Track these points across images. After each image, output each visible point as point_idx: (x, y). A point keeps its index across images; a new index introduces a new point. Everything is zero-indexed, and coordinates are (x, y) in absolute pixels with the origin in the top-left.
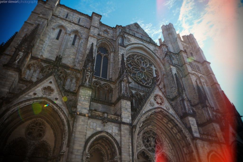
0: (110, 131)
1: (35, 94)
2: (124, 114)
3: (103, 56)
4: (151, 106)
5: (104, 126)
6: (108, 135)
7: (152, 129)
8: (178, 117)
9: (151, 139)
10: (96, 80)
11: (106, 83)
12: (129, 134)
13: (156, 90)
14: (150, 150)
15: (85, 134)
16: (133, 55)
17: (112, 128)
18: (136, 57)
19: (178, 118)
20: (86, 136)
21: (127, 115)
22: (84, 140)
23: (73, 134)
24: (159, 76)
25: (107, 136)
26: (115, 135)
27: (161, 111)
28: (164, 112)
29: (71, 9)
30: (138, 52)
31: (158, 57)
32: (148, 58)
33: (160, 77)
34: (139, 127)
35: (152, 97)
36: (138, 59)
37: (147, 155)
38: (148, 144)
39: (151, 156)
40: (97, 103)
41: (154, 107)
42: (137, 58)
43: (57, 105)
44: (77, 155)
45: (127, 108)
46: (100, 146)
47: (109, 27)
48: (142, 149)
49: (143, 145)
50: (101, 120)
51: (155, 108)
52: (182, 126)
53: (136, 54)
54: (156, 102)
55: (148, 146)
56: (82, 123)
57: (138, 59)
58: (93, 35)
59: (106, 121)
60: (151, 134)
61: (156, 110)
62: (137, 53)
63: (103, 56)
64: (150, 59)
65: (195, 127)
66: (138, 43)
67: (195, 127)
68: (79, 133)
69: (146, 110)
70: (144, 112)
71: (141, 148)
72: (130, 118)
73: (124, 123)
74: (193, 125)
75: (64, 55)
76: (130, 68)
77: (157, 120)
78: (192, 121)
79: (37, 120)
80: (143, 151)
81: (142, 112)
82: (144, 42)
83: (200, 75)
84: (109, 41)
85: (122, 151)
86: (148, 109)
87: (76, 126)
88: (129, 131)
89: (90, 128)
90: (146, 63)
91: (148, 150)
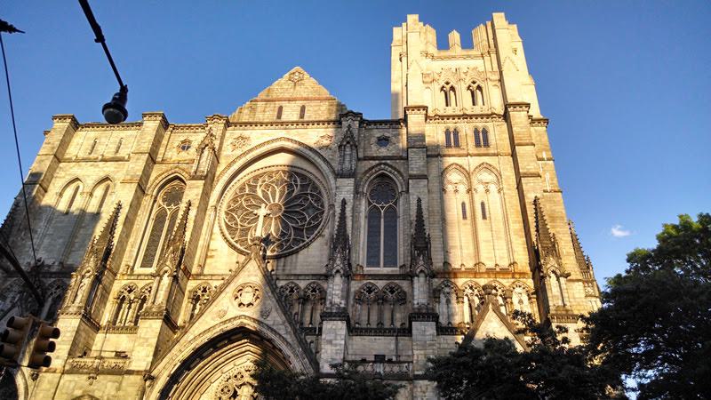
5: (91, 384)
8: (289, 329)
13: (247, 273)
16: (256, 179)
19: (287, 333)
24: (323, 212)
33: (325, 214)
35: (228, 295)
50: (87, 373)
51: (224, 322)
52: (294, 353)
54: (236, 303)
56: (48, 386)
58: (132, 176)
63: (169, 213)
65: (336, 345)
67: (336, 345)
69: (197, 333)
70: (192, 337)
72: (150, 359)
73: (130, 372)
74: (330, 342)
75: (74, 245)
78: (335, 331)
83: (475, 161)
84: (183, 170)
89: (62, 393)
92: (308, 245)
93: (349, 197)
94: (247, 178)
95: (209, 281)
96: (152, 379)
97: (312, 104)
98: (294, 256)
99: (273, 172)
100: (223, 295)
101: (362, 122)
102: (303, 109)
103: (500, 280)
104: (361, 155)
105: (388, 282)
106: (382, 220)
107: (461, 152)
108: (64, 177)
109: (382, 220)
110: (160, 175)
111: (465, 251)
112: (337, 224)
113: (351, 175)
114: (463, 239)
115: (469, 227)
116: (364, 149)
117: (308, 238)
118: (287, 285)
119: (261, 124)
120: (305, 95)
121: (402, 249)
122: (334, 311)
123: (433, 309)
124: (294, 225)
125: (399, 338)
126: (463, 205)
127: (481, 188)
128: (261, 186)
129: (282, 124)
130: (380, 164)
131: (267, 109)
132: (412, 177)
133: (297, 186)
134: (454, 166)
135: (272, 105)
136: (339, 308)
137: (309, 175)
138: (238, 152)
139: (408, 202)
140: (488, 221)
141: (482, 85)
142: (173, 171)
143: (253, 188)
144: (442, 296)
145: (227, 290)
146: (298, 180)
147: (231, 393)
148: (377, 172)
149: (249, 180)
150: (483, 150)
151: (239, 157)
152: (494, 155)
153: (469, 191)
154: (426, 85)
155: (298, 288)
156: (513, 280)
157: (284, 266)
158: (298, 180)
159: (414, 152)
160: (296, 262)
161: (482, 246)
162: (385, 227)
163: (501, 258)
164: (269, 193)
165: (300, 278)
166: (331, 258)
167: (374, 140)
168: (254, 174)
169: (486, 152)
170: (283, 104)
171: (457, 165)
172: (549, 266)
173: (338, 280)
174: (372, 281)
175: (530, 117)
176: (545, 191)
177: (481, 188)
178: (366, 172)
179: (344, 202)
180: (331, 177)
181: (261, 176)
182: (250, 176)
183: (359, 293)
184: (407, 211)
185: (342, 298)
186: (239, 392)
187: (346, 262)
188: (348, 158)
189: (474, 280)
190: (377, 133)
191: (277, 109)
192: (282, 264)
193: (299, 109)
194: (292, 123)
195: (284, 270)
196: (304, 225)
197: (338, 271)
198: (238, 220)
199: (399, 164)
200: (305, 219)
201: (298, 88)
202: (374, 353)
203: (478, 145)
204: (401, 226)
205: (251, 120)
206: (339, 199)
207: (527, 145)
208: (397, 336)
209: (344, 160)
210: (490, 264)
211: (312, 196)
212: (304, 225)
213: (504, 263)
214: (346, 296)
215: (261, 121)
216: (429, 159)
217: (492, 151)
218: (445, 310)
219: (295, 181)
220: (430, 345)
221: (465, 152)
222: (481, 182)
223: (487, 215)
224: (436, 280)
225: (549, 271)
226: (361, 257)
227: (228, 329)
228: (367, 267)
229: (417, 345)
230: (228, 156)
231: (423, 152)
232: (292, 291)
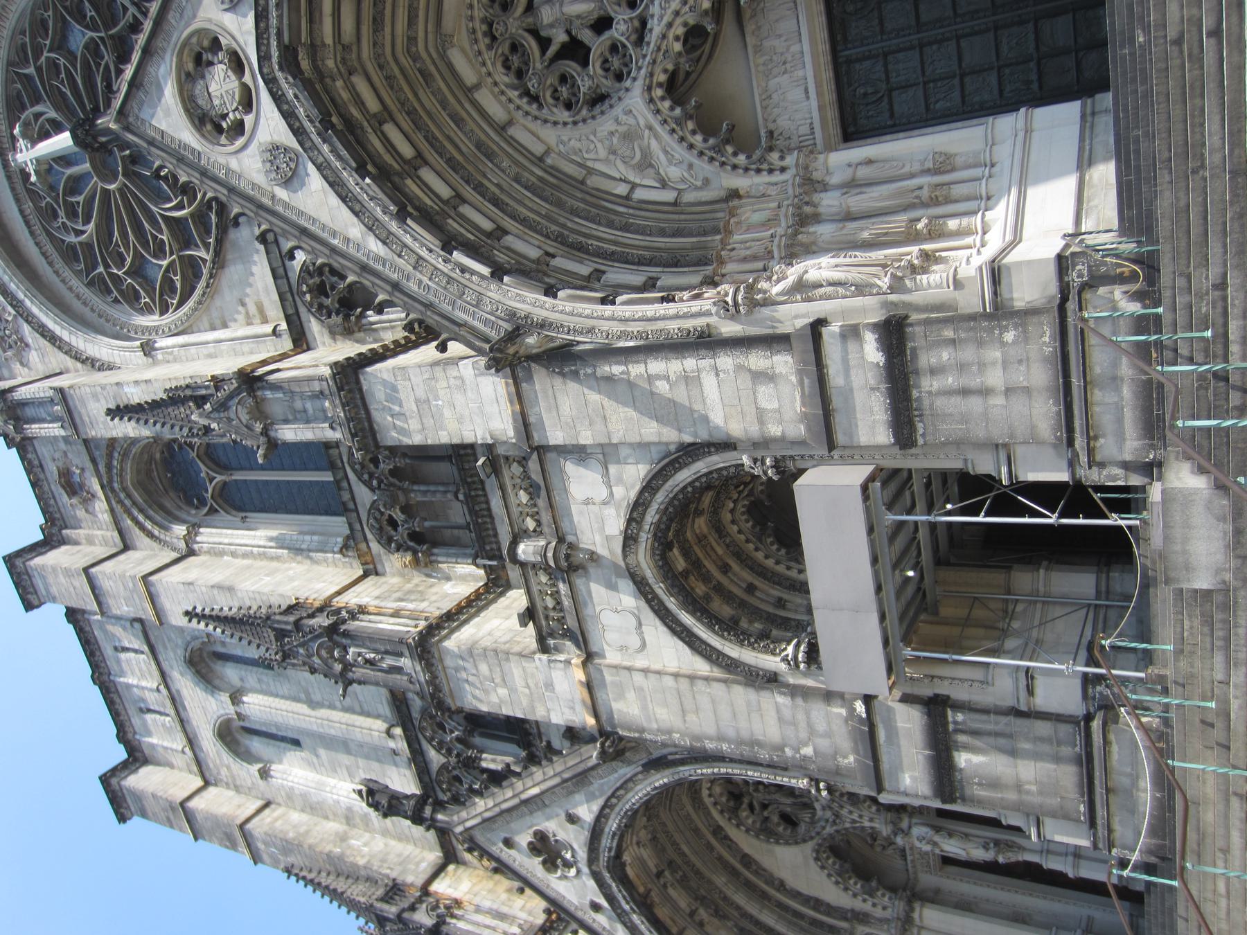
0: (615, 524)
1: (596, 907)
2: (460, 420)
3: (219, 478)
6: (638, 534)
7: (474, 31)
9: (551, 26)
10: (370, 536)
11: (354, 470)
12: (572, 386)
14: (636, 23)
15: (684, 684)
16: (69, 254)
17: (588, 502)
20: (692, 678)
21: (459, 399)
22: (719, 689)
23: (710, 745)
25: (645, 538)
26: (620, 480)
27: (289, 61)
28: (279, 34)
29: (110, 704)
34: (493, 286)
35: (234, 164)
36: (72, 212)
37: (678, 47)
38: (597, 45)
39: (677, 13)
40: (493, 523)
41: (292, 142)
43: (601, 818)
44: (810, 725)
45: (417, 401)
46: (731, 505)
47: (29, 471)
48: (650, 117)
49: (618, 110)
51: (298, 132)
55: (614, 48)
56: (631, 695)
59: (563, 550)
60: (513, 24)
61: (307, 124)
62: (38, 229)
63: (219, 478)
68: (691, 718)
69: (355, 230)
70: (374, 246)
71: (650, 128)
73: (525, 424)
76: (167, 270)
77: (377, 23)
79: (715, 804)
80: (659, 92)
81: (377, 258)
85: (703, 436)
86: (334, 200)
87: (658, 730)
88: (558, 381)
91: (640, 40)
94: (74, 282)
95: (294, 278)
96: (514, 335)
99: (38, 208)
108: (228, 767)
110: (142, 528)
117: (125, 9)
128: (79, 233)
133: (38, 116)
142: (122, 496)
147: (571, 67)
149: (78, 274)
164: (81, 199)
168: (59, 264)
181: (58, 243)
182: (67, 273)
186: (560, 37)
196: (101, 38)
198: (165, 263)
200: (93, 48)
211: (38, 53)
227: (314, 112)
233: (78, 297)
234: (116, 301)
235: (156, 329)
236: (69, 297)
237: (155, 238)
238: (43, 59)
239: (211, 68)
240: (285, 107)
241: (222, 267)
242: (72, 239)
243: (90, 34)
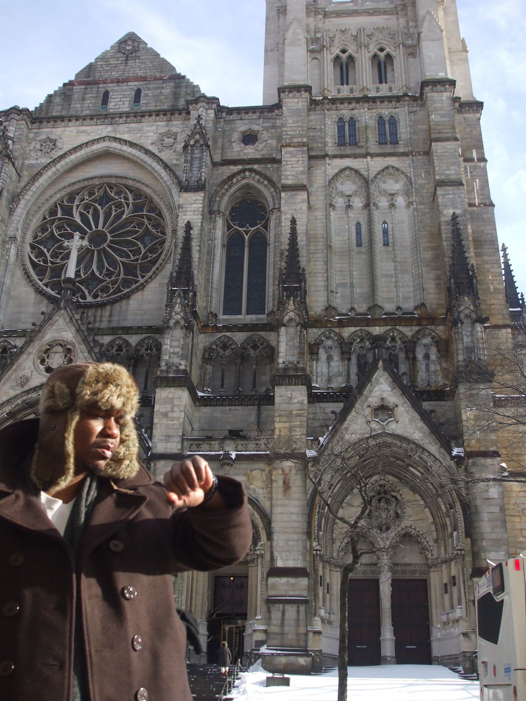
4: (17, 388)
16: (71, 198)
18: (82, 200)
24: (164, 242)
30: (88, 179)
31: (166, 166)
32: (130, 183)
35: (31, 356)
36: (87, 207)
41: (26, 388)
42: (85, 201)
51: (28, 392)
53: (83, 188)
54: (42, 367)
57: (87, 207)
61: (30, 396)
62: (86, 183)
64: (138, 185)
65: (173, 419)
66: (86, 143)
67: (173, 419)
82: (121, 121)
90: (119, 205)
92: (143, 287)
93: (196, 219)
94: (58, 196)
97: (151, 86)
98: (124, 302)
99: (95, 186)
100: (24, 356)
101: (221, 111)
102: (138, 93)
103: (401, 328)
104: (217, 158)
105: (250, 333)
106: (246, 250)
107: (358, 151)
109: (246, 250)
111: (357, 290)
112: (179, 257)
113: (199, 187)
114: (355, 273)
115: (364, 257)
116: (223, 149)
117: (143, 277)
118: (113, 341)
119: (77, 118)
120: (140, 73)
121: (271, 290)
122: (171, 375)
123: (304, 369)
124: (123, 260)
125: (263, 407)
126: (358, 225)
127: (383, 203)
128: (78, 206)
129: (106, 116)
130: (244, 171)
131: (87, 96)
132: (287, 188)
133: (128, 205)
134: (347, 172)
135: (96, 90)
136: (178, 371)
137: (145, 189)
138: (45, 161)
139: (279, 224)
140: (390, 248)
141: (393, 53)
143: (68, 211)
144: (321, 351)
145: (30, 349)
146: (130, 196)
148: (238, 181)
150: (388, 149)
151: (47, 167)
152: (405, 154)
153: (367, 206)
154: (314, 55)
155: (128, 344)
156: (417, 328)
157: (110, 316)
158: (130, 196)
159: (290, 152)
160: (127, 310)
161: (381, 283)
162: (250, 258)
163: (406, 299)
165: (130, 332)
166: (170, 305)
167: (236, 136)
169: (393, 151)
170: (110, 87)
171: (351, 169)
172: (462, 308)
173: (178, 333)
174: (228, 334)
175: (456, 99)
176: (471, 205)
177: (383, 203)
178: (224, 182)
179: (189, 226)
180: (175, 191)
182: (63, 193)
183: (208, 350)
184: (278, 236)
185: (183, 357)
187: (188, 310)
188: (196, 164)
189: (366, 328)
190: (242, 126)
191: (101, 95)
192: (108, 313)
193: (133, 93)
194: (121, 115)
195: (110, 321)
197: (177, 323)
198: (48, 255)
199: (269, 169)
200: (138, 251)
201: (131, 63)
202: (229, 427)
203: (382, 142)
204: (272, 257)
205: (64, 113)
206: (182, 223)
207: (447, 139)
208: (259, 405)
209: (192, 164)
210: (389, 307)
211: (149, 219)
212: (137, 260)
213: (409, 305)
214: (188, 355)
215: (79, 114)
216: (313, 162)
217: (402, 150)
218: (325, 370)
219: (126, 199)
220: (297, 415)
221: (362, 151)
222: (384, 193)
223: (391, 241)
224: (315, 330)
225: (462, 316)
226: (214, 301)
228: (224, 314)
229: (280, 416)
230: (31, 166)
231: (303, 152)
232: (120, 348)
233: (51, 197)
234: (45, 218)
235: (23, 242)
236: (50, 192)
237: (61, 254)
238: (145, 220)
239: (63, 357)
240: (37, 389)
241: (36, 291)
242: (76, 202)
243: (143, 253)
